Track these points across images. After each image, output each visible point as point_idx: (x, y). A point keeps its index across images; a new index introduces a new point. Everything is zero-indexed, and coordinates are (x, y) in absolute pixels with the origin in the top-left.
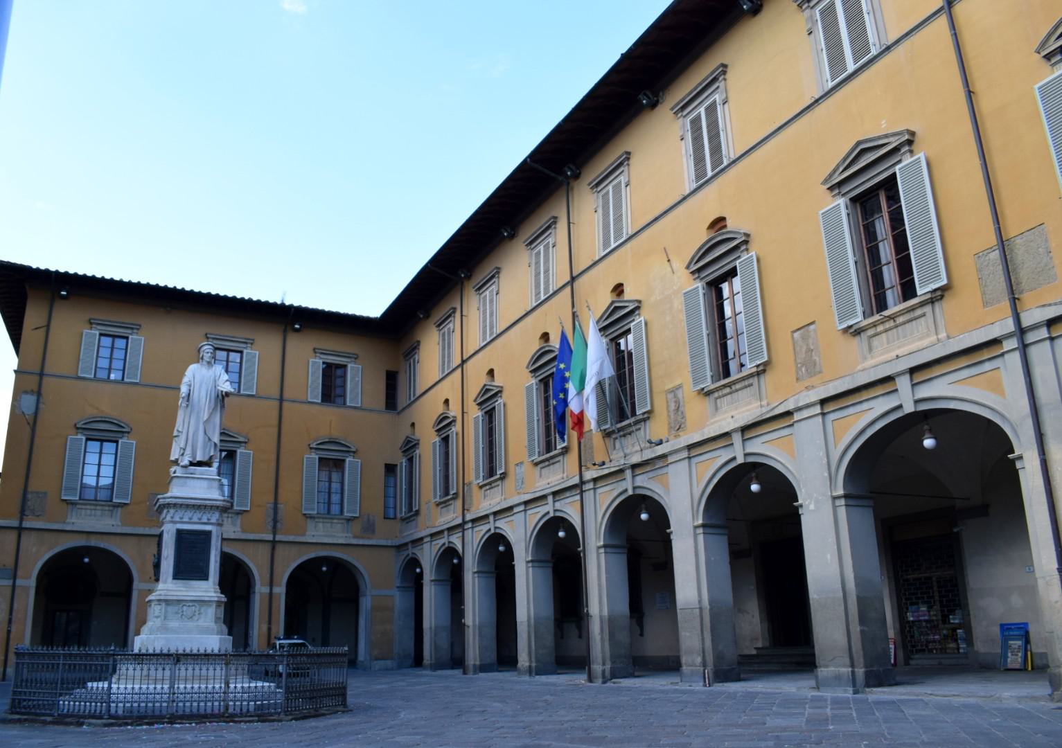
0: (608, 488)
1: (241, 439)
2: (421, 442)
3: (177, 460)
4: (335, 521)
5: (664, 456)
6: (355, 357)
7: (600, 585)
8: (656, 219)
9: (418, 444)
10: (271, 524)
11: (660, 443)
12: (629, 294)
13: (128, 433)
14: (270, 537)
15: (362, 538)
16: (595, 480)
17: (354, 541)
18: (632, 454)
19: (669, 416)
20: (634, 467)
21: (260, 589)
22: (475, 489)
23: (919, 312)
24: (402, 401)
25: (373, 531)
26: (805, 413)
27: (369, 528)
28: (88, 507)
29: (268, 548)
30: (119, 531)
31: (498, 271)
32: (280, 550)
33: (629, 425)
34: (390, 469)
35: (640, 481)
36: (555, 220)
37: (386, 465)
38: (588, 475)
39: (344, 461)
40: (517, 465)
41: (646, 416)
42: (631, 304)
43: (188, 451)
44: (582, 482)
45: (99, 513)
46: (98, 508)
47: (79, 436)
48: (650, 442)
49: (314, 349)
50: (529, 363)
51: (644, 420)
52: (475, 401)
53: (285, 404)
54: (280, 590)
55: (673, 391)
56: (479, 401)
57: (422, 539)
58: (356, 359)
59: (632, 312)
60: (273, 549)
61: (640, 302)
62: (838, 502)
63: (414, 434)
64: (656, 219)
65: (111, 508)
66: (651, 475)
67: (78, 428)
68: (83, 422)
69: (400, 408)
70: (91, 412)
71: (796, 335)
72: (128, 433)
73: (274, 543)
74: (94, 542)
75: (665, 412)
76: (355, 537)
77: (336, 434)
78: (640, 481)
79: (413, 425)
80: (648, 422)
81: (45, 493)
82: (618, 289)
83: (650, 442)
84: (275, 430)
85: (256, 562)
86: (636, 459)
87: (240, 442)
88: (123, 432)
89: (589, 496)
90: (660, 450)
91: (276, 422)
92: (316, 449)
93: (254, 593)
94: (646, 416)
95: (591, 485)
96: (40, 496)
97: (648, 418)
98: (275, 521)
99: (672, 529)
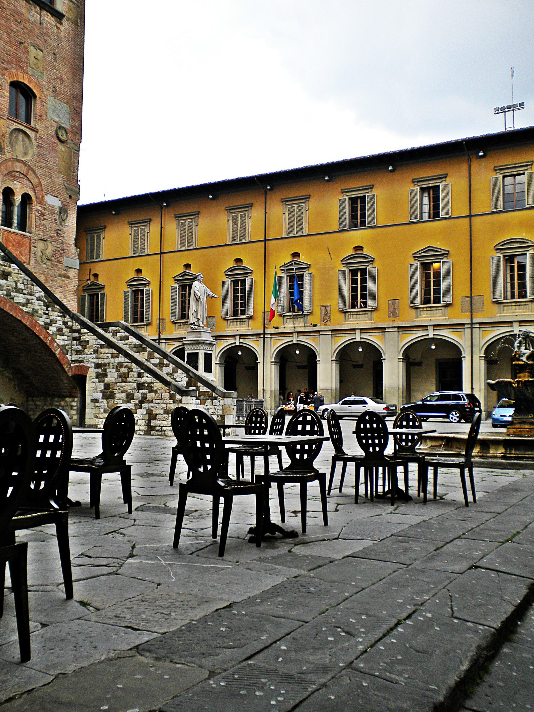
2: (106, 287)
5: (319, 331)
7: (271, 378)
8: (325, 233)
9: (104, 288)
11: (315, 325)
12: (302, 259)
16: (271, 334)
19: (321, 316)
20: (298, 333)
22: (168, 324)
23: (440, 308)
26: (391, 330)
31: (198, 213)
35: (301, 338)
36: (251, 206)
38: (267, 331)
43: (201, 320)
44: (264, 334)
48: (311, 324)
52: (174, 278)
55: (325, 307)
56: (176, 278)
62: (399, 360)
64: (325, 233)
66: (308, 337)
71: (390, 302)
75: (320, 314)
78: (301, 338)
82: (296, 255)
83: (311, 324)
86: (303, 330)
89: (268, 340)
90: (315, 329)
95: (269, 336)
99: (318, 359)
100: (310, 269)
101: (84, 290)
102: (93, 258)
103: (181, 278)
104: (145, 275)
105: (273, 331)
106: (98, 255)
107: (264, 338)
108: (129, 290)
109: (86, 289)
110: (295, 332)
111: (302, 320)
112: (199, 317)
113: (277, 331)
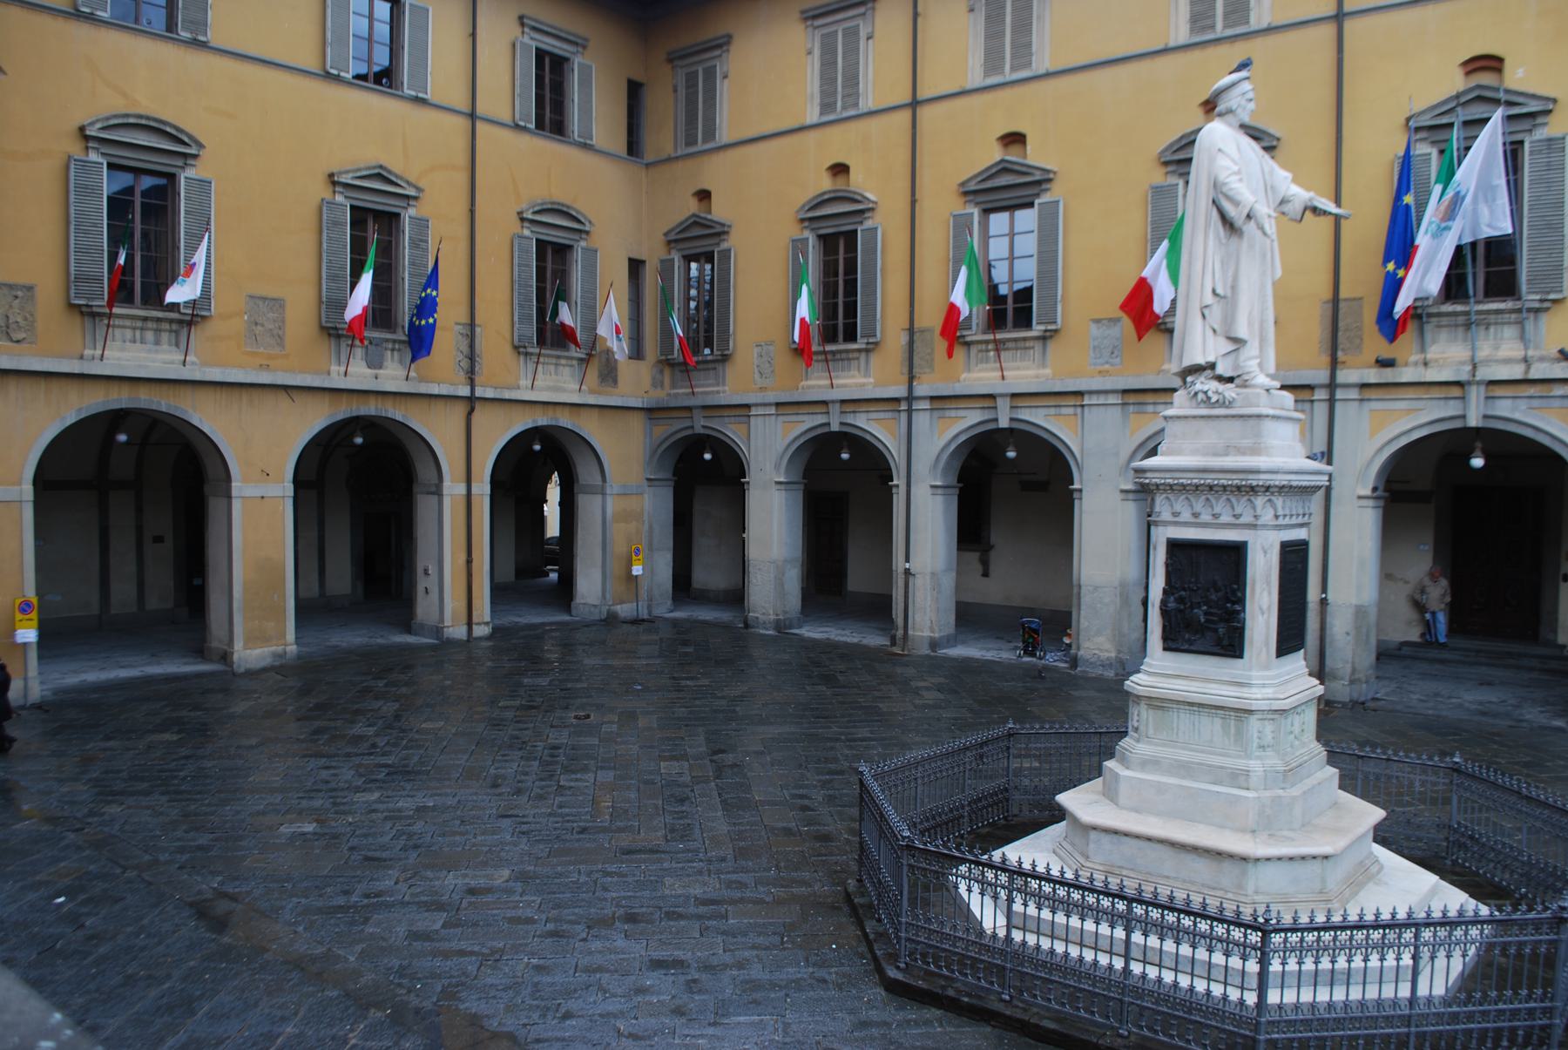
0: (1420, 404)
1: (412, 192)
3: (1212, 366)
4: (563, 362)
6: (580, 44)
9: (727, 233)
10: (465, 364)
13: (195, 157)
14: (464, 391)
15: (599, 393)
17: (591, 400)
18: (1488, 361)
21: (453, 488)
24: (661, 136)
25: (615, 382)
27: (609, 374)
28: (128, 323)
29: (460, 411)
30: (198, 376)
32: (481, 417)
33: (1498, 312)
34: (635, 266)
37: (631, 260)
39: (570, 247)
40: (1097, 321)
41: (1546, 305)
42: (1533, 102)
44: (1332, 386)
45: (150, 335)
46: (150, 324)
47: (93, 156)
49: (521, 18)
50: (1171, 145)
51: (1537, 311)
53: (480, 126)
54: (482, 488)
57: (748, 406)
58: (584, 47)
59: (1532, 115)
60: (470, 413)
61: (1555, 101)
63: (710, 212)
65: (174, 327)
66: (1536, 403)
67: (87, 138)
68: (99, 125)
69: (650, 157)
70: (113, 104)
72: (195, 157)
73: (472, 401)
74: (145, 399)
76: (592, 392)
77: (560, 195)
79: (704, 196)
80: (1544, 317)
81: (30, 288)
84: (462, 178)
85: (440, 432)
87: (408, 197)
88: (185, 155)
91: (462, 159)
92: (532, 222)
93: (438, 492)
94: (1546, 305)
96: (19, 293)
97: (1547, 309)
98: (472, 357)
100: (1551, 119)
101: (669, 242)
102: (695, 143)
103: (989, 184)
104: (858, 181)
105: (1373, 375)
106: (710, 133)
107: (1332, 401)
108: (807, 234)
109: (676, 241)
110: (1479, 383)
111: (1509, 332)
112: (1242, 331)
113: (1388, 375)
